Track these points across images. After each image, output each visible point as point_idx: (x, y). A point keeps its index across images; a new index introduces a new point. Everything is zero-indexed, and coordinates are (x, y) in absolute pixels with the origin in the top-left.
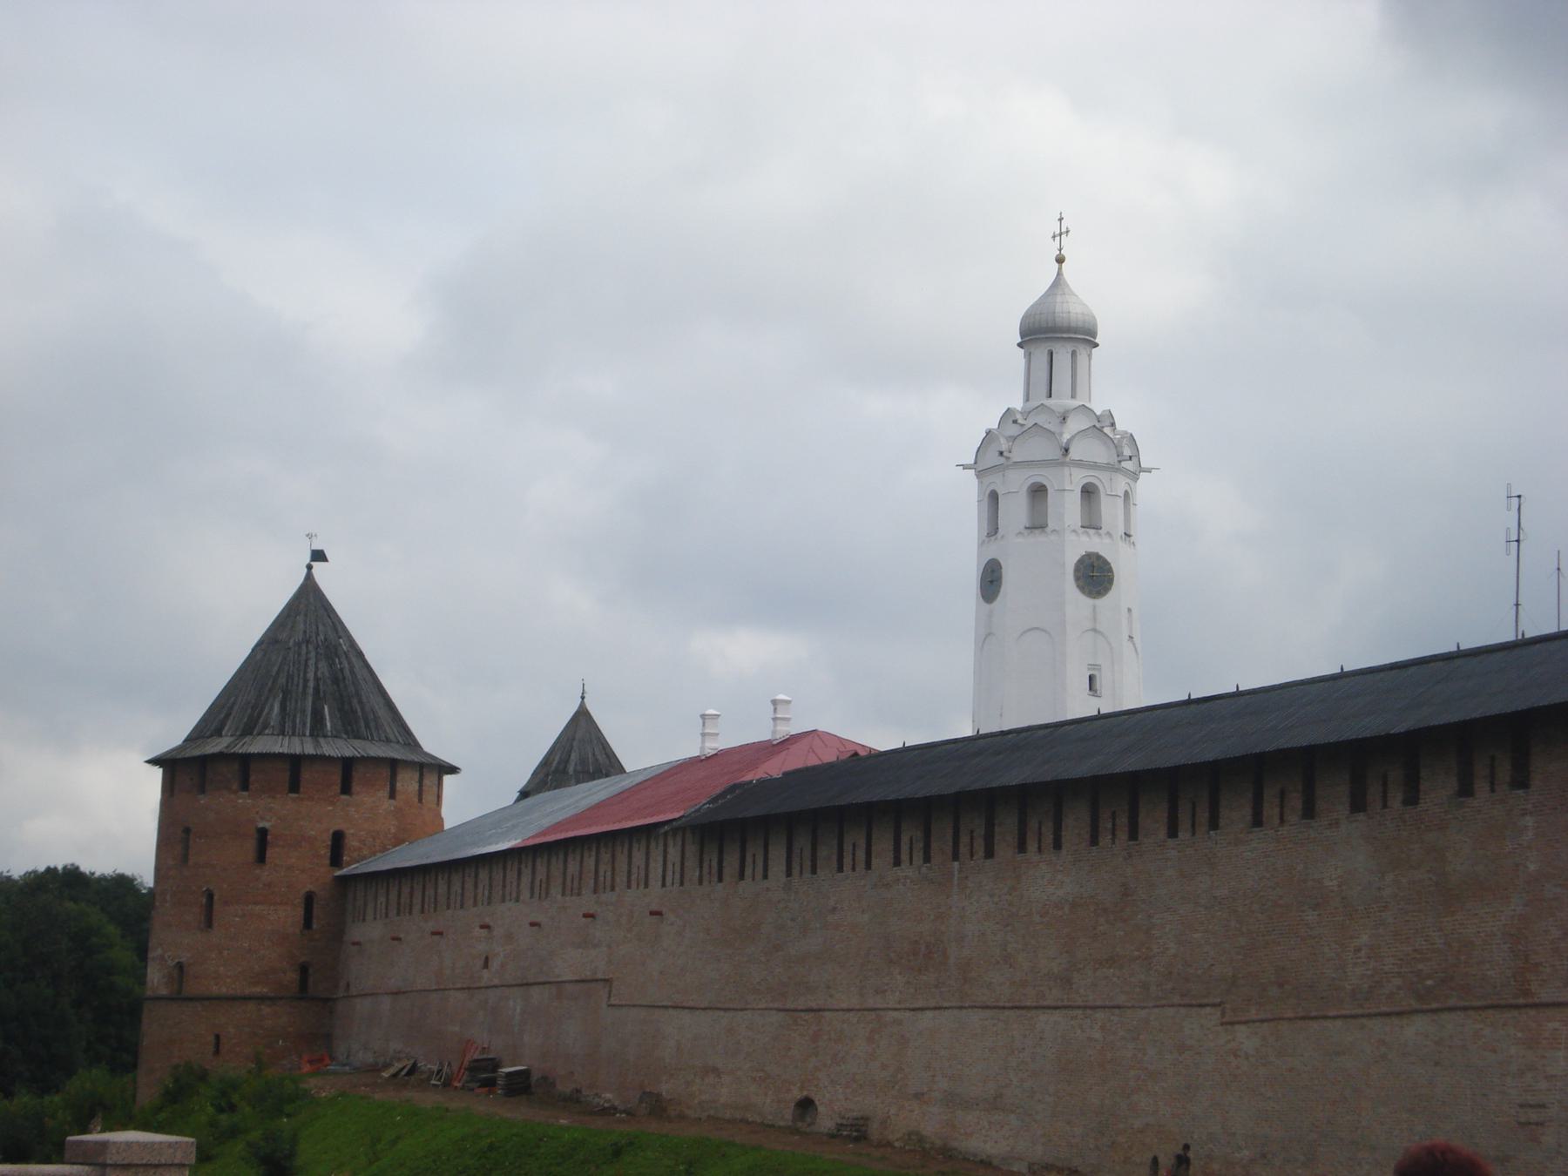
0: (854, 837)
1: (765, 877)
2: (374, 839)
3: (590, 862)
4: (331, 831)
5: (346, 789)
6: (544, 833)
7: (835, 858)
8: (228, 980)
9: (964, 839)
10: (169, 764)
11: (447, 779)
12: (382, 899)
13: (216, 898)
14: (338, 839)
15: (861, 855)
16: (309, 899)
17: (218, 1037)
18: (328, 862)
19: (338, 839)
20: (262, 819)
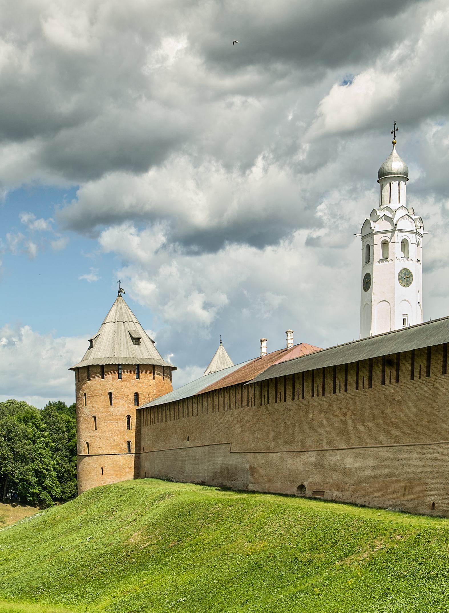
0: (340, 378)
1: (285, 401)
2: (149, 395)
3: (210, 402)
4: (134, 393)
5: (138, 377)
6: (202, 391)
7: (311, 391)
8: (104, 448)
9: (361, 381)
10: (77, 370)
11: (172, 372)
12: (152, 417)
13: (97, 419)
14: (137, 394)
15: (321, 391)
16: (129, 417)
17: (102, 468)
18: (133, 404)
19: (137, 394)
20: (110, 389)
